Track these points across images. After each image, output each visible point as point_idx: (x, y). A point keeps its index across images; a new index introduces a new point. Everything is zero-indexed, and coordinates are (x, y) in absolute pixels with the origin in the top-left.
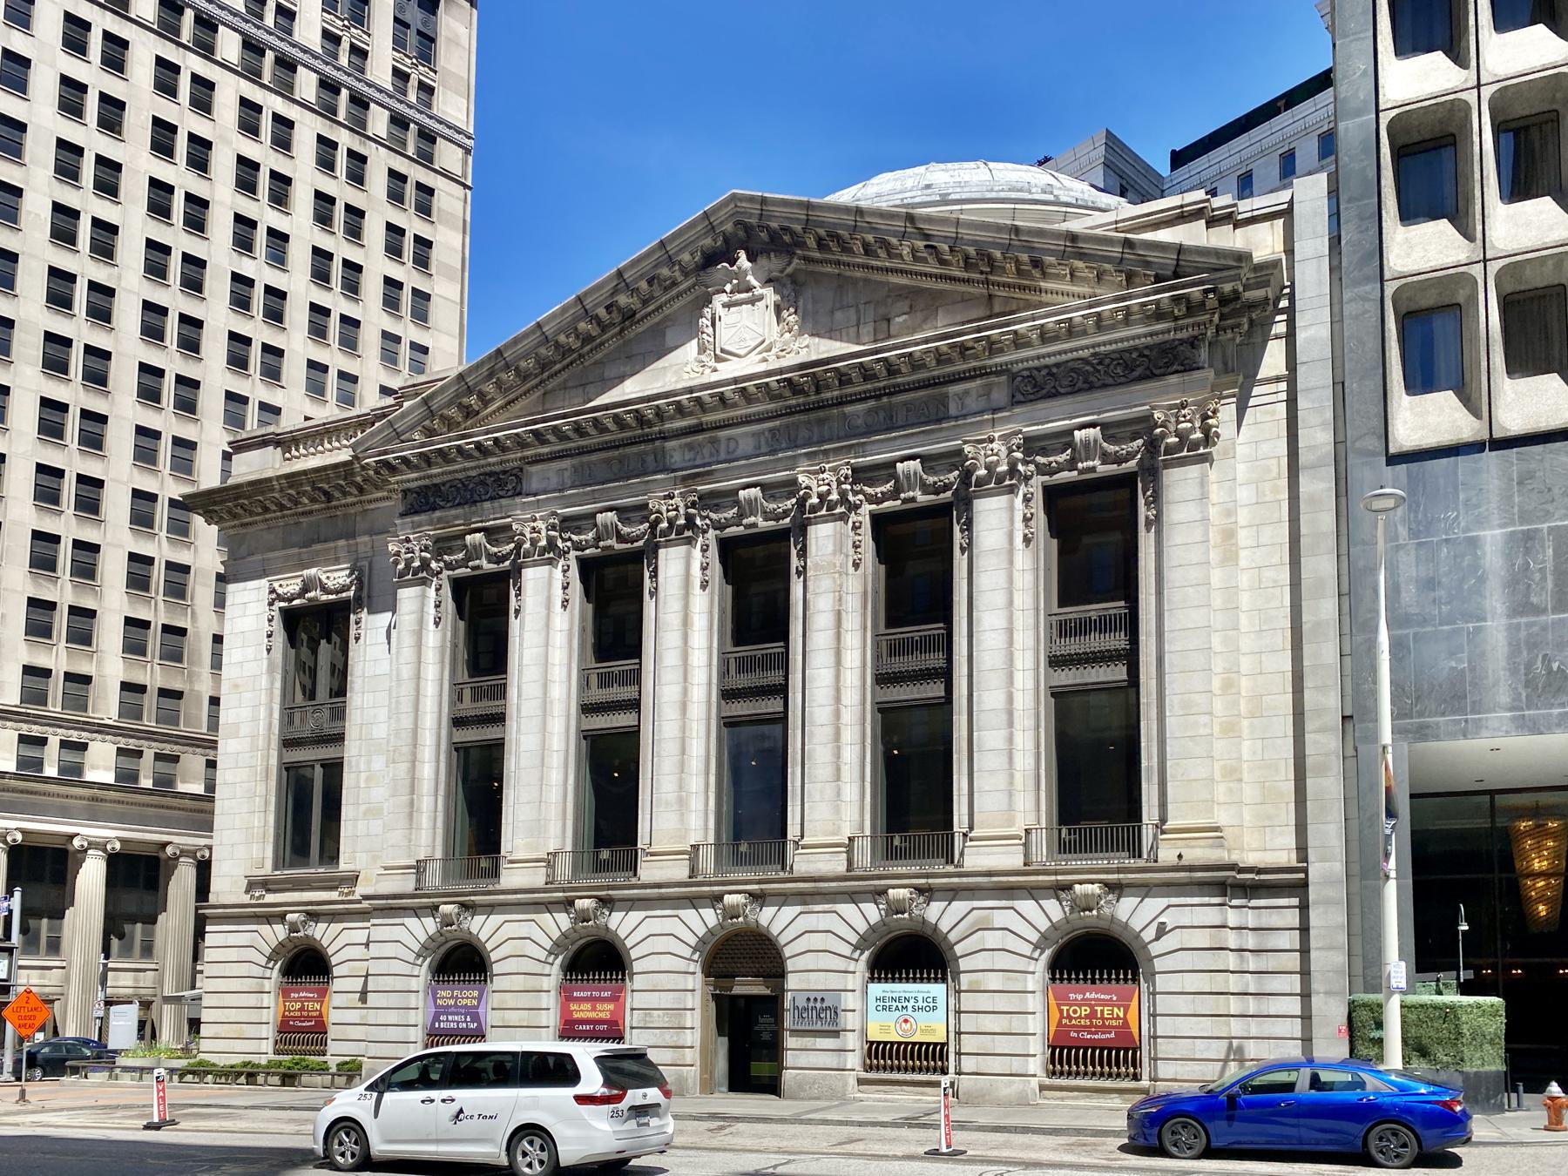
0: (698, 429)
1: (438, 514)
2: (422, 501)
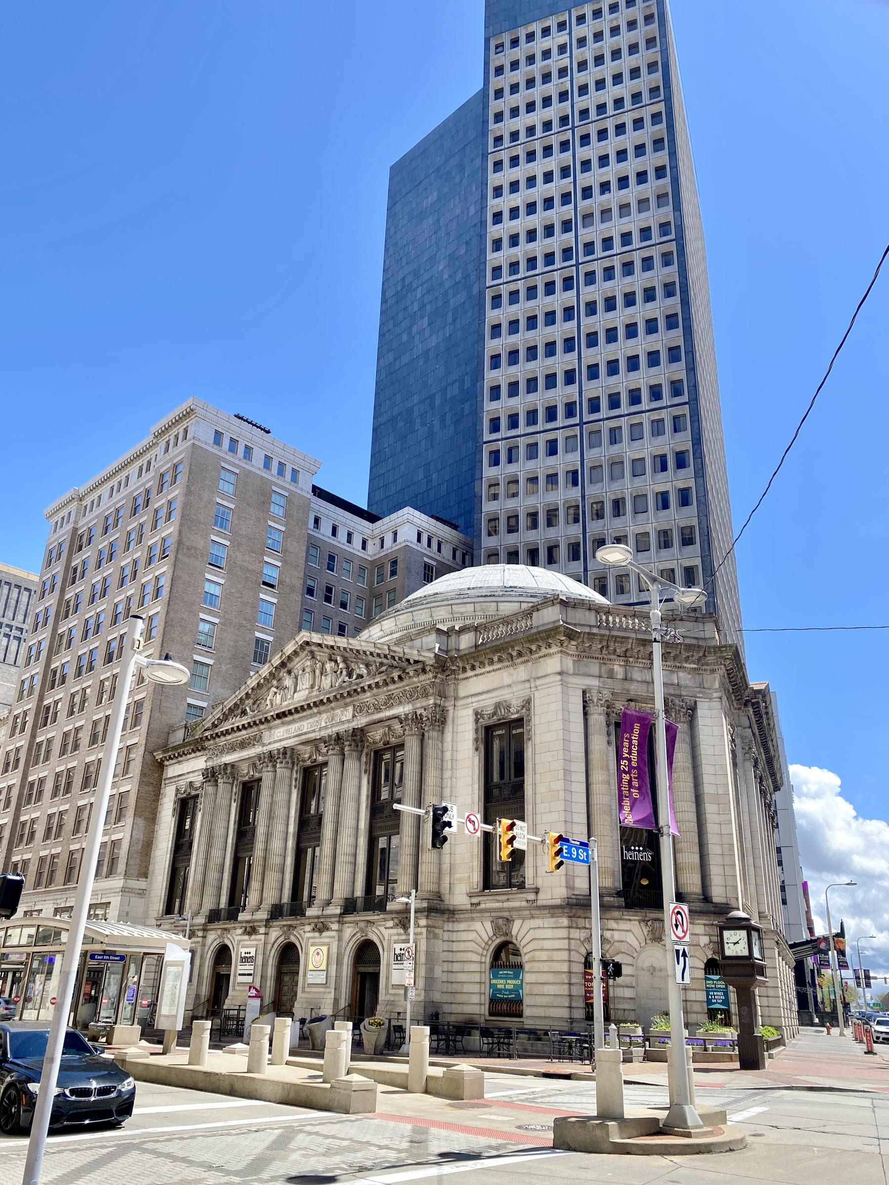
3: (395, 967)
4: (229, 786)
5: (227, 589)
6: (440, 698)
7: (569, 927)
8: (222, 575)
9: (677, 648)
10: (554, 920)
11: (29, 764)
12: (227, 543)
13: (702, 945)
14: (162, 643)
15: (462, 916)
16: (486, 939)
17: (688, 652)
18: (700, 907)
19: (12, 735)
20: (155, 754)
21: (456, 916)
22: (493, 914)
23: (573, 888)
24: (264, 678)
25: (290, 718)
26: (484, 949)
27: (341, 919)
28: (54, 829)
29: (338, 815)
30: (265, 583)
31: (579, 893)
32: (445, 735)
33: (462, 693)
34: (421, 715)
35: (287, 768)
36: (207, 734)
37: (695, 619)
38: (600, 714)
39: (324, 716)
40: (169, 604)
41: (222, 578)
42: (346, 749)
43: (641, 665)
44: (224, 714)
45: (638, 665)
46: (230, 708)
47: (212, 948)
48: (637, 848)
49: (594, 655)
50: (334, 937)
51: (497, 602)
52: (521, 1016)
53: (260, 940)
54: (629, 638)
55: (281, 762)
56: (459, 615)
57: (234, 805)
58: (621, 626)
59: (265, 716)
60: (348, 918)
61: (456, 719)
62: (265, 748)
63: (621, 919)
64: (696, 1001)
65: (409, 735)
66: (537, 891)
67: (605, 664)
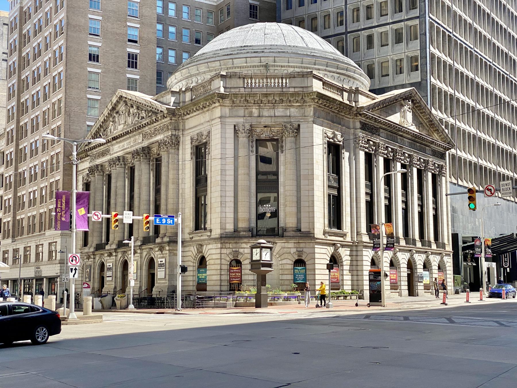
0: (401, 136)
1: (367, 133)
2: (364, 127)
3: (158, 270)
4: (102, 177)
5: (103, 49)
6: (174, 131)
7: (221, 248)
8: (99, 40)
10: (216, 245)
11: (18, 161)
12: (100, 18)
13: (292, 253)
14: (66, 90)
15: (188, 244)
16: (195, 255)
17: (293, 97)
19: (8, 144)
20: (70, 157)
21: (185, 244)
22: (196, 243)
23: (225, 229)
24: (106, 116)
25: (118, 140)
26: (194, 260)
27: (140, 248)
28: (21, 204)
29: (140, 194)
30: (130, 41)
31: (228, 231)
32: (179, 151)
33: (187, 127)
34: (166, 141)
35: (121, 167)
36: (87, 148)
37: (302, 76)
38: (243, 137)
39: (132, 139)
40: (66, 65)
41: (100, 42)
42: (141, 158)
43: (268, 107)
44: (92, 136)
45: (266, 107)
46: (94, 133)
47: (98, 264)
48: (267, 206)
49: (240, 105)
50: (138, 256)
51: (232, 59)
52: (205, 290)
53: (114, 259)
55: (118, 165)
56: (213, 69)
57: (105, 187)
58: (259, 85)
59: (108, 139)
60: (144, 247)
61: (184, 142)
62: (112, 156)
64: (287, 280)
65: (163, 152)
66: (211, 231)
67: (248, 109)
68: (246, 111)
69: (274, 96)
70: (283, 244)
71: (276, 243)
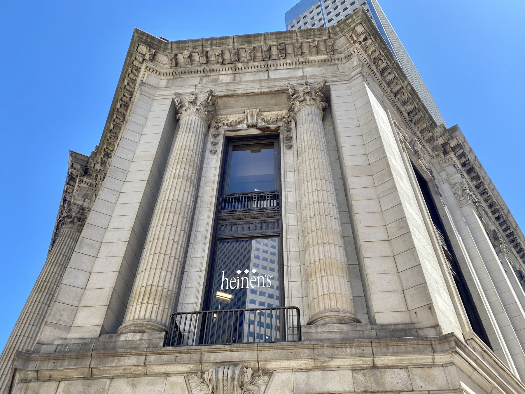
9: (291, 37)
18: (341, 332)
45: (250, 70)
54: (228, 38)
63: (146, 375)
67: (209, 76)
68: (205, 80)
69: (265, 39)
70: (302, 376)
71: (269, 373)
